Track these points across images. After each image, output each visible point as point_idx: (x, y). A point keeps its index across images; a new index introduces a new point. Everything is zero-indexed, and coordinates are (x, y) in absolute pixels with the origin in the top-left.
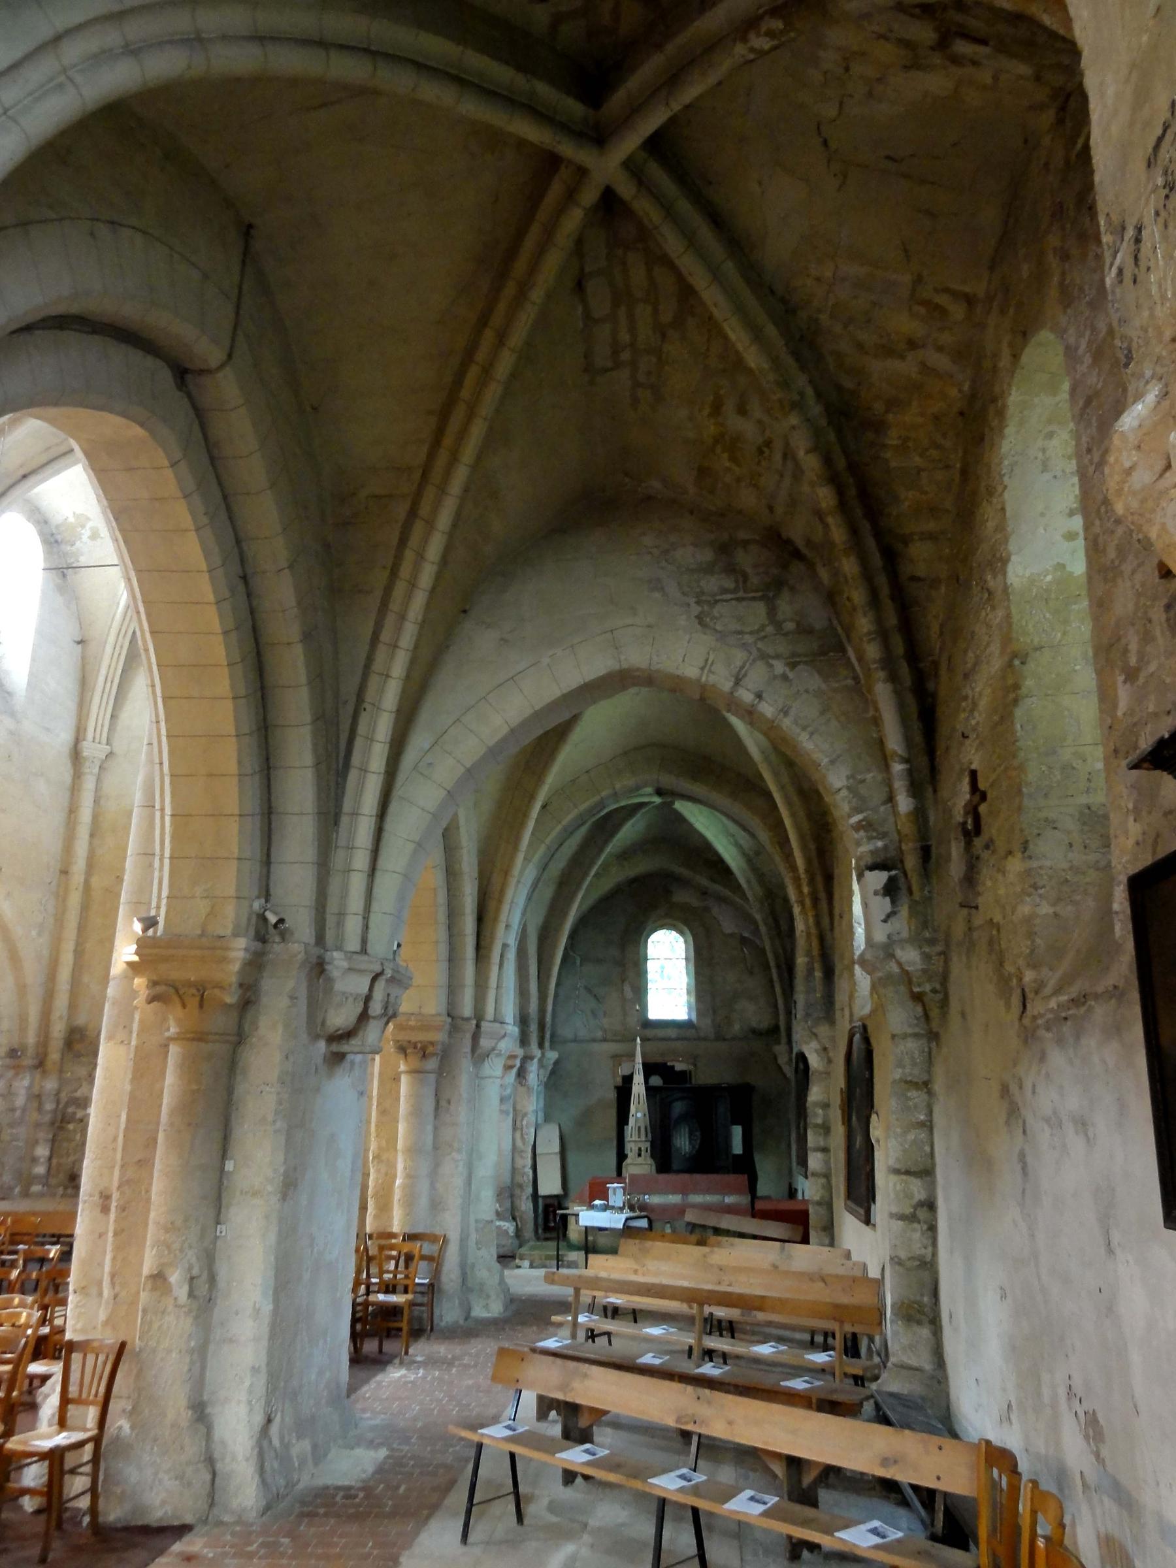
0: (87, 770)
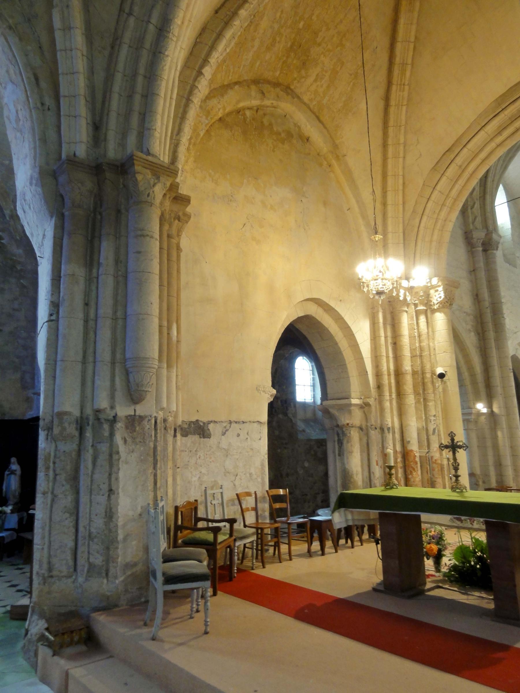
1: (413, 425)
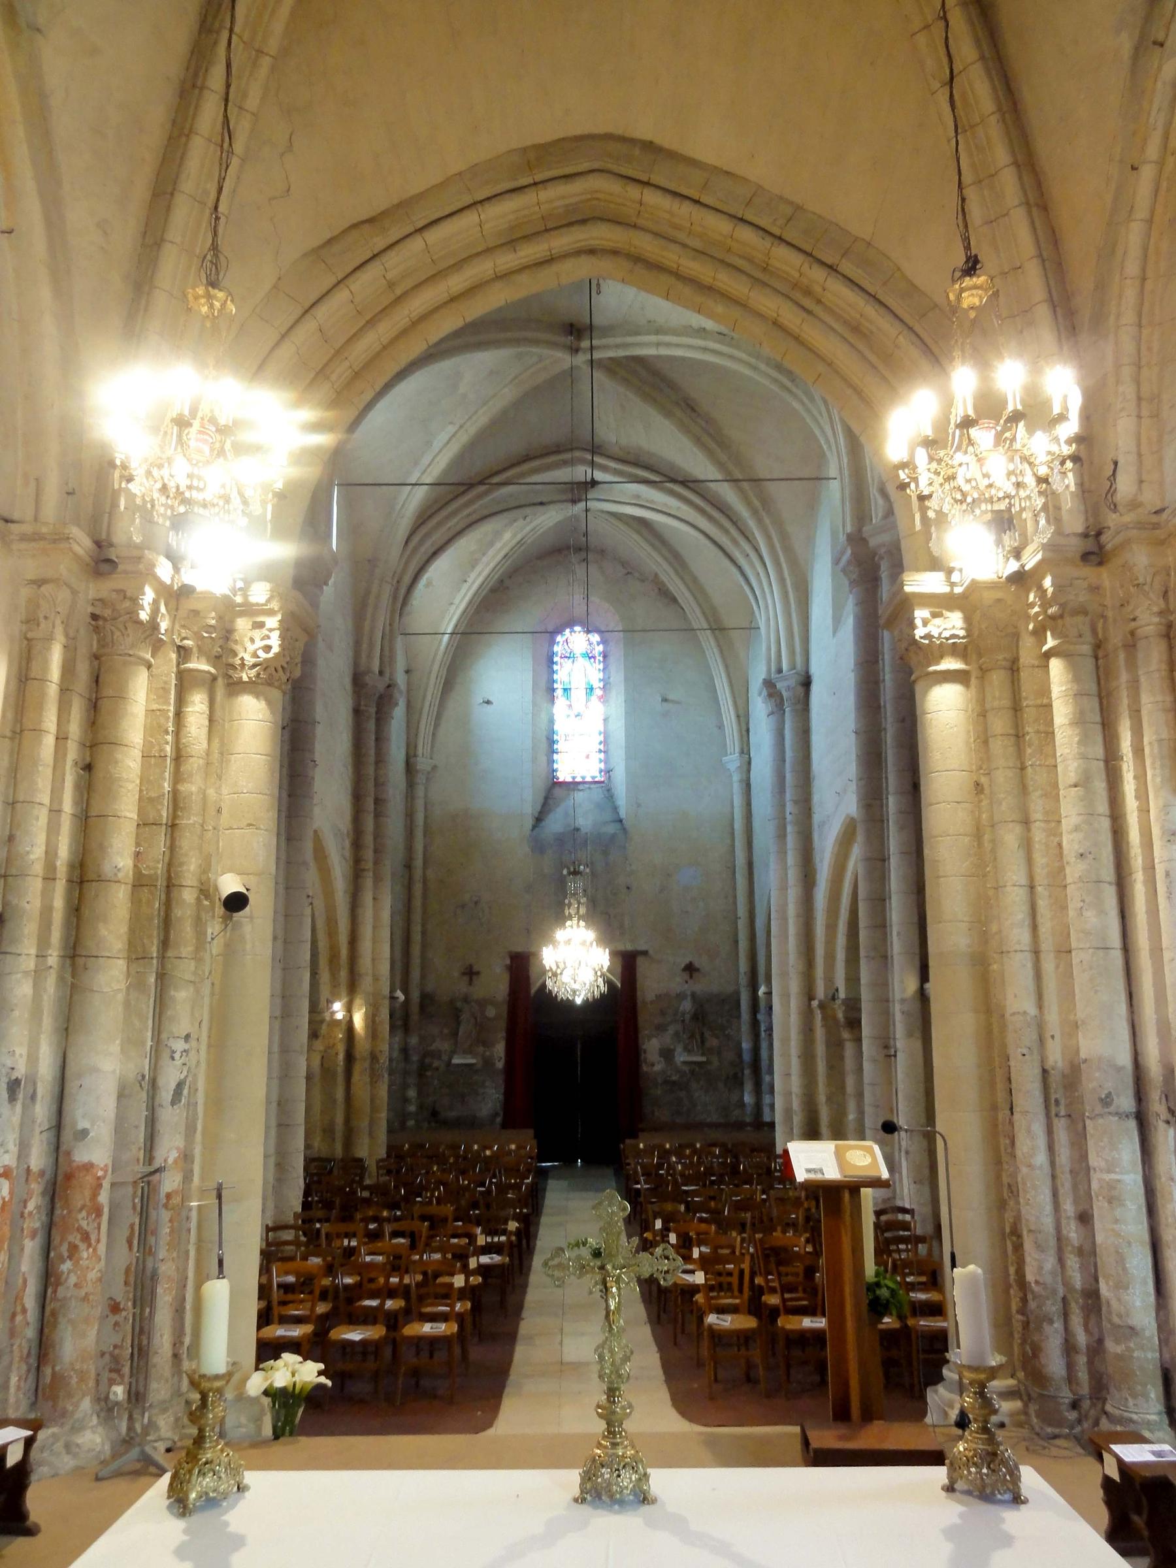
1: (107, 1064)
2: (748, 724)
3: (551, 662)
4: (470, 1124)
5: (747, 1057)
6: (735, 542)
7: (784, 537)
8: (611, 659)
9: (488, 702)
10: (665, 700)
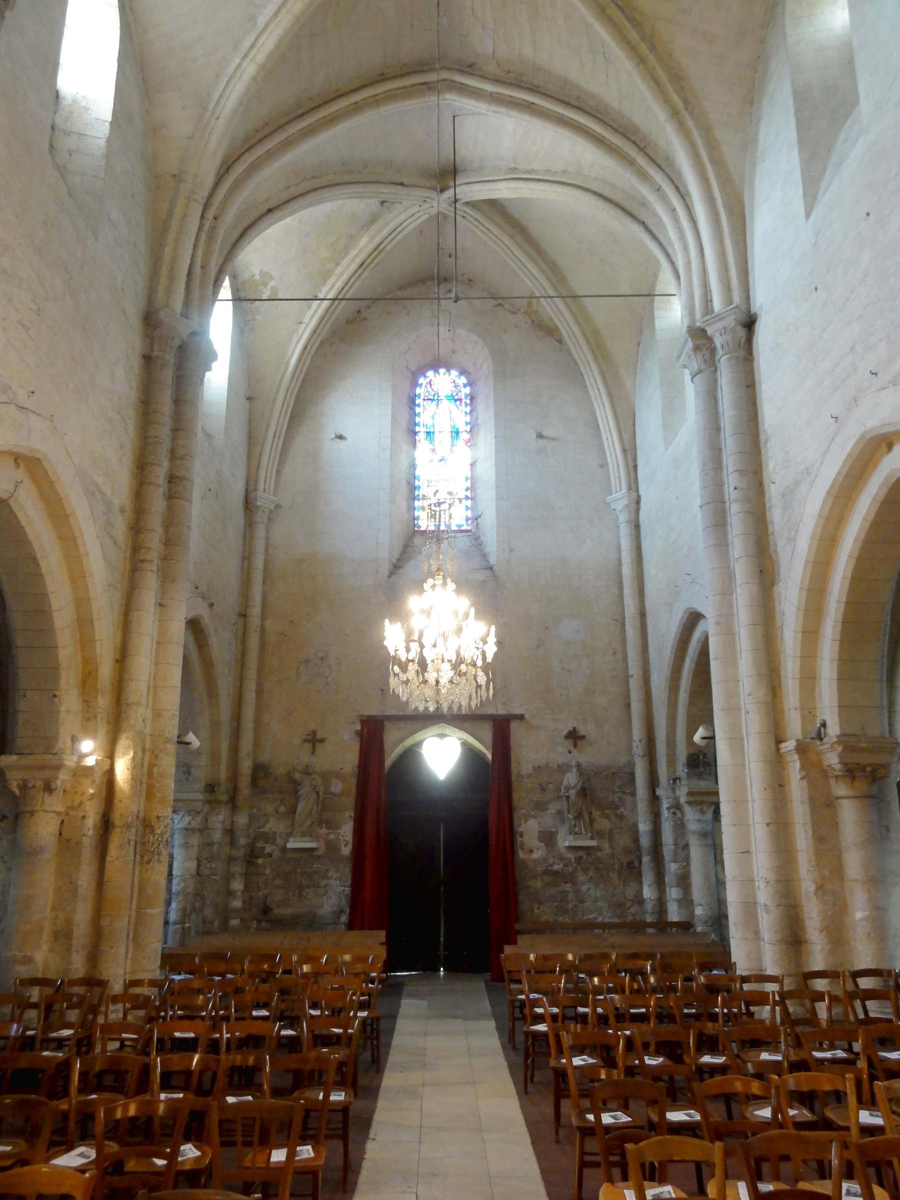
0: (259, 519)
2: (635, 459)
3: (412, 402)
4: (309, 923)
5: (645, 842)
6: (644, 176)
7: (712, 146)
8: (480, 400)
9: (341, 437)
10: (540, 436)
